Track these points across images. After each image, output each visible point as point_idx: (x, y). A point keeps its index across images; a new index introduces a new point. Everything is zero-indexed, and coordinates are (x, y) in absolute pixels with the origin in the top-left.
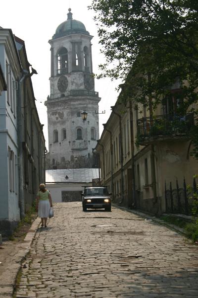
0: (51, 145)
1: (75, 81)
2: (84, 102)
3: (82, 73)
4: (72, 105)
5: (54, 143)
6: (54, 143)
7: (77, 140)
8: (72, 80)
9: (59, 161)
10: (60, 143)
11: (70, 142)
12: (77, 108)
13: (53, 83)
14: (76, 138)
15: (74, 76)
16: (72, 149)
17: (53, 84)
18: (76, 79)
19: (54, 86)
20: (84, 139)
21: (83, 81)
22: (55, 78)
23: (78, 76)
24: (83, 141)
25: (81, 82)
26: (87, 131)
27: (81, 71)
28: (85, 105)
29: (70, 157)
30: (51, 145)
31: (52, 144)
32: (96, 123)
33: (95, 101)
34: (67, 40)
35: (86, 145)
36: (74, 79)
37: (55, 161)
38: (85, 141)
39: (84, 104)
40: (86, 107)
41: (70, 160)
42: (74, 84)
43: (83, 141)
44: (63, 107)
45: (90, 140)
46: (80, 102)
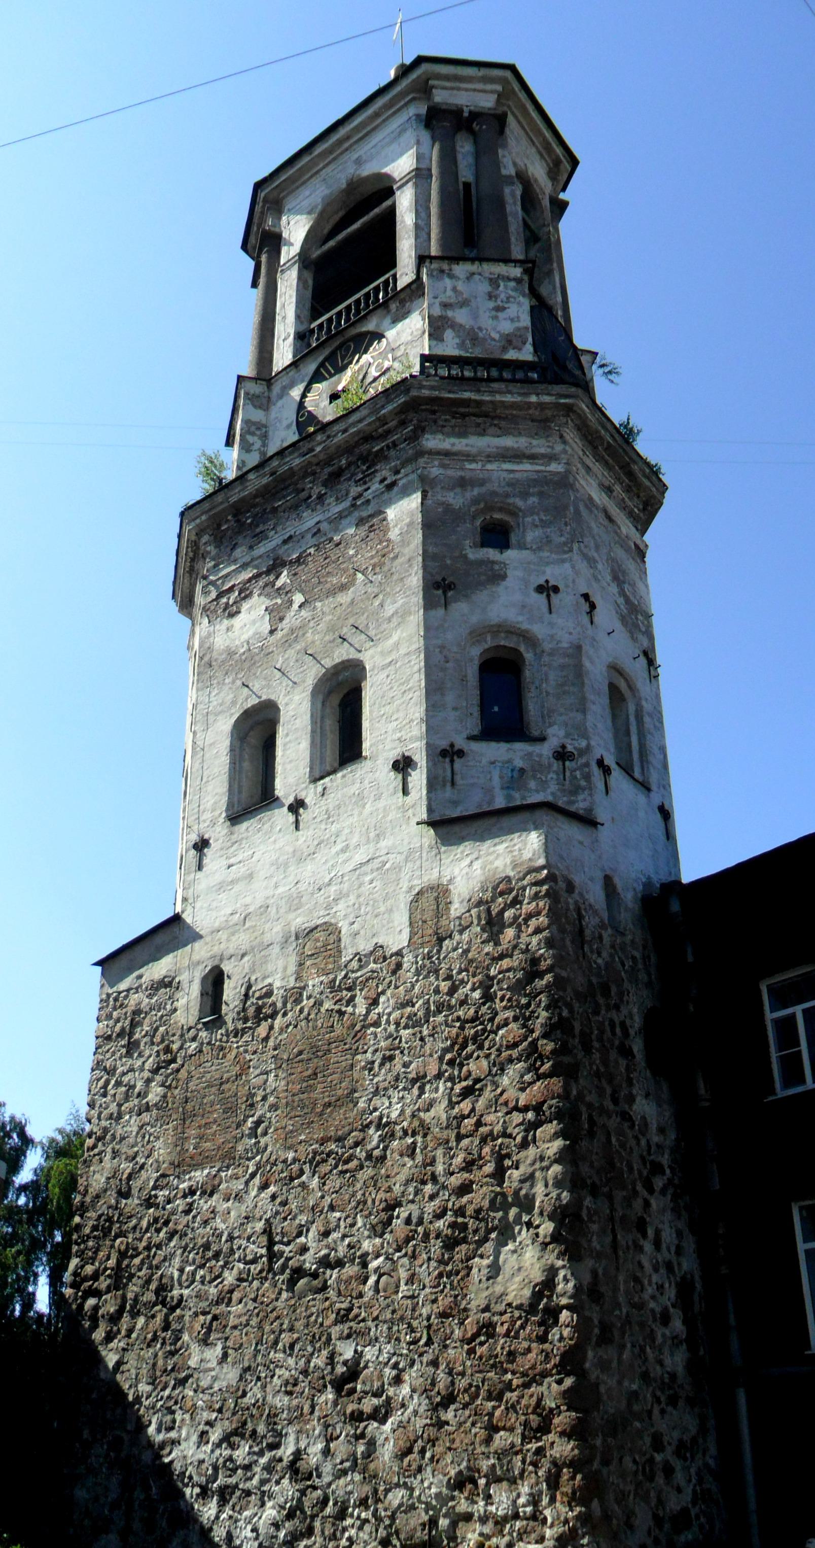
0: (201, 845)
1: (461, 316)
2: (540, 446)
3: (517, 272)
4: (447, 454)
5: (235, 818)
6: (235, 818)
7: (472, 738)
8: (437, 311)
9: (277, 984)
10: (297, 806)
11: (403, 765)
12: (482, 483)
13: (258, 415)
14: (473, 724)
15: (448, 282)
16: (432, 823)
17: (260, 426)
18: (464, 303)
19: (265, 437)
20: (556, 736)
21: (526, 321)
22: (276, 388)
23: (485, 287)
24: (545, 750)
25: (507, 327)
26: (579, 672)
27: (507, 261)
28: (554, 467)
29: (401, 919)
30: (201, 845)
31: (218, 833)
32: (643, 660)
33: (617, 488)
34: (395, 124)
35: (576, 790)
36: (445, 306)
37: (231, 993)
38: (562, 755)
39: (551, 458)
40: (564, 482)
41: (397, 937)
42: (449, 334)
43: (545, 750)
44: (346, 504)
45: (609, 761)
46: (508, 442)
